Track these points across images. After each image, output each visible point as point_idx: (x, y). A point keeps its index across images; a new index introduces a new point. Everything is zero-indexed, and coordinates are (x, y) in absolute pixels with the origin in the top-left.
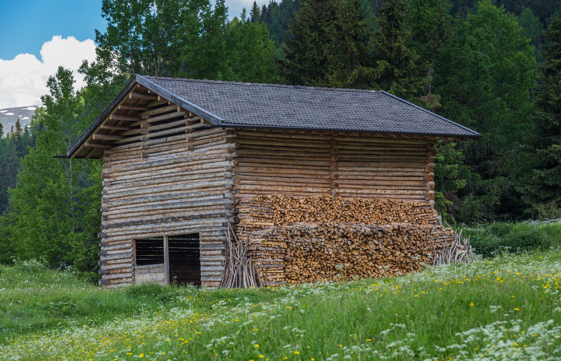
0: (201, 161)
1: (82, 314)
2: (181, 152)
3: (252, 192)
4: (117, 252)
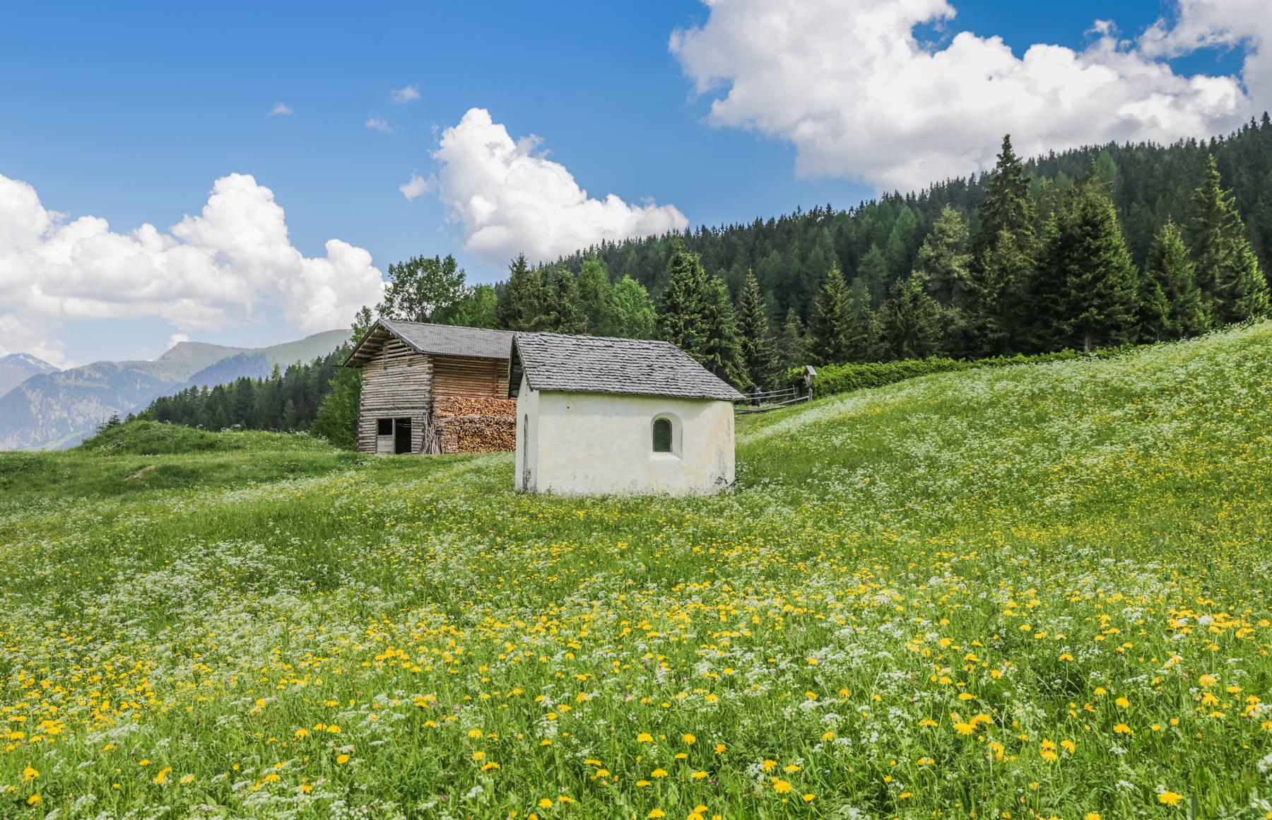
0: (414, 374)
1: (303, 470)
2: (404, 368)
3: (443, 394)
4: (368, 427)
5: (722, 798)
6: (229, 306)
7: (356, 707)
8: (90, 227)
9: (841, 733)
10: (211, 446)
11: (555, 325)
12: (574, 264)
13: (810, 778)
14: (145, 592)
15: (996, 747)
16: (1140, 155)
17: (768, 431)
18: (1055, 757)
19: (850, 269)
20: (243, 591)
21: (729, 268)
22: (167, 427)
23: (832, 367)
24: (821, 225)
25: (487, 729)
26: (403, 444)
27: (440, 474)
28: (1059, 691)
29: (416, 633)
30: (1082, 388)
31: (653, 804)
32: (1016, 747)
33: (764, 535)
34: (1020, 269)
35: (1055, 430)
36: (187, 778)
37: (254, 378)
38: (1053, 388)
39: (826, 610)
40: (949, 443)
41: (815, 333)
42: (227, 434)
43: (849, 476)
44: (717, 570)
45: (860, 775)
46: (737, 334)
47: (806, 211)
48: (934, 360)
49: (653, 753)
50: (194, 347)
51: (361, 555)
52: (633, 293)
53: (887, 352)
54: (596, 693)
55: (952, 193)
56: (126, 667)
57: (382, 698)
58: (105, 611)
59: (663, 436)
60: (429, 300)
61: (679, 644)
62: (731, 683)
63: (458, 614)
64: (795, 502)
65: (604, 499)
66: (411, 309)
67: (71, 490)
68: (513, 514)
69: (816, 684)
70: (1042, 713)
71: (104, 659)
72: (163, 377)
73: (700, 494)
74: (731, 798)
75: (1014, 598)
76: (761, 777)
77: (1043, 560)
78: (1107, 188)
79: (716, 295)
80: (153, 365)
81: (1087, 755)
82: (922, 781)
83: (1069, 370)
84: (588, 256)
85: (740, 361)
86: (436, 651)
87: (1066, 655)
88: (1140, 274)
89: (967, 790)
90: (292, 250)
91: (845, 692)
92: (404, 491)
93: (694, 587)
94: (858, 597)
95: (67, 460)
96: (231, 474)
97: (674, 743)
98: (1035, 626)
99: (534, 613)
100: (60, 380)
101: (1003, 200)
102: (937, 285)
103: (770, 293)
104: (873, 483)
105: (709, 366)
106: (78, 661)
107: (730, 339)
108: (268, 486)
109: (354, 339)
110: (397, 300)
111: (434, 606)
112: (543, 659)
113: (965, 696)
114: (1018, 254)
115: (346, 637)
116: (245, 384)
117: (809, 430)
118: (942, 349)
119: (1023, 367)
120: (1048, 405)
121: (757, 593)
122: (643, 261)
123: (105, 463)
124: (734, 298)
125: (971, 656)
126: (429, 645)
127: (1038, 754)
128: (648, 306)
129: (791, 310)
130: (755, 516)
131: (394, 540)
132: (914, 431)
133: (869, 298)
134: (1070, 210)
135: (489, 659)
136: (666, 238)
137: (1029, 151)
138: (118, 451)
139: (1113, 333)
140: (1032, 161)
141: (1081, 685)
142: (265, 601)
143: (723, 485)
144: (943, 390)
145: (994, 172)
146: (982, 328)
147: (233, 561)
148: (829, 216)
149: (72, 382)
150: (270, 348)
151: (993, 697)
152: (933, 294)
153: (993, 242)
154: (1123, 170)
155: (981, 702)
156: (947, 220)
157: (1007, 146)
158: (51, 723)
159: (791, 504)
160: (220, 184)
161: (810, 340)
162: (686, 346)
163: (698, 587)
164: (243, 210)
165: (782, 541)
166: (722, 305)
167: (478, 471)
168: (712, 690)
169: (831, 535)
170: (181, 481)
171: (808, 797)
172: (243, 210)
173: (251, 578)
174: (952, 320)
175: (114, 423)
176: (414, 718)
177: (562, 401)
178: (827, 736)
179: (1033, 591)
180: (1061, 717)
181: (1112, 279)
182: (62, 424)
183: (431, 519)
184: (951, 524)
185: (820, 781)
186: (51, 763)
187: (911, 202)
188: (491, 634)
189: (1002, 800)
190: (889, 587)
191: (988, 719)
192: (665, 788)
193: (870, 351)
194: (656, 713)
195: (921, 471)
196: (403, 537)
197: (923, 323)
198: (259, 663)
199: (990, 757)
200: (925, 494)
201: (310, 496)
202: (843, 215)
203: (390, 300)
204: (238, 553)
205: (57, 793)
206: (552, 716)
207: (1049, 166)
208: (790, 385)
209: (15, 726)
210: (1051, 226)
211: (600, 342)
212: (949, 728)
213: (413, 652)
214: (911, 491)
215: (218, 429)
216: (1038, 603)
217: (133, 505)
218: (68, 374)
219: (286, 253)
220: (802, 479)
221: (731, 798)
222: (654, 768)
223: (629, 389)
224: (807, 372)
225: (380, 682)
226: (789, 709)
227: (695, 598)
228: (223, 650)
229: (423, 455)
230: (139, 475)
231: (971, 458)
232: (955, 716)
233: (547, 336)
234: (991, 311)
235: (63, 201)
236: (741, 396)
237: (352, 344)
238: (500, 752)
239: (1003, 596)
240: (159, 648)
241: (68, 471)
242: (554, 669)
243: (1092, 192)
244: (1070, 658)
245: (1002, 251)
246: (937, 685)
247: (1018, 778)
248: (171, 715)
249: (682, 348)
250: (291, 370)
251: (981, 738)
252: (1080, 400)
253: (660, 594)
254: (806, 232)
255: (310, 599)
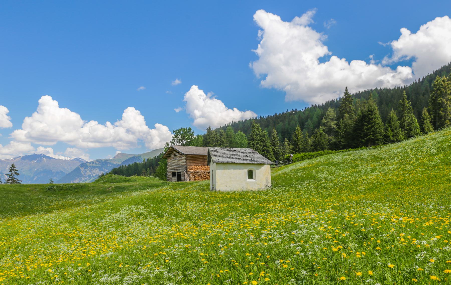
2: (178, 158)
5: (269, 269)
6: (131, 143)
7: (170, 248)
8: (93, 123)
9: (301, 252)
10: (128, 181)
11: (220, 145)
12: (225, 128)
13: (293, 264)
14: (114, 219)
15: (344, 255)
16: (384, 91)
17: (280, 172)
18: (360, 256)
19: (302, 126)
20: (139, 218)
21: (268, 127)
22: (115, 176)
23: (298, 154)
24: (294, 114)
25: (205, 253)
26: (179, 179)
27: (190, 187)
28: (361, 239)
29: (185, 229)
30: (368, 157)
31: (250, 271)
32: (349, 254)
33: (279, 200)
34: (350, 125)
35: (360, 169)
36: (127, 266)
37: (138, 162)
38: (360, 157)
39: (296, 219)
40: (331, 174)
41: (292, 145)
42: (133, 177)
43: (302, 184)
44: (267, 210)
45: (306, 262)
46: (271, 146)
47: (289, 111)
48: (326, 151)
49: (250, 258)
50: (122, 154)
51: (169, 209)
52: (241, 136)
53: (313, 149)
54: (234, 243)
55: (331, 104)
56: (110, 238)
57: (177, 245)
58: (104, 224)
59: (251, 175)
60: (184, 139)
61: (256, 230)
62: (271, 240)
63: (196, 223)
64: (288, 191)
65: (235, 192)
66: (180, 142)
67: (93, 193)
68: (210, 197)
69: (294, 239)
70: (357, 245)
71: (105, 236)
72: (115, 163)
73: (261, 190)
74: (271, 269)
75: (349, 215)
76: (280, 264)
77: (357, 204)
78: (375, 101)
79: (264, 136)
80: (112, 160)
81: (368, 255)
82: (323, 264)
83: (364, 152)
84: (228, 126)
85: (272, 153)
86: (190, 233)
87: (363, 229)
88: (384, 125)
89: (336, 266)
90: (147, 127)
91: (302, 241)
92: (179, 192)
93: (260, 215)
94: (305, 216)
95: (91, 185)
96: (134, 188)
97: (256, 256)
98: (355, 222)
99: (216, 223)
100: (88, 164)
101: (346, 105)
102: (327, 130)
103: (280, 134)
104: (309, 185)
105: (263, 155)
106: (98, 236)
107: (269, 147)
108: (144, 191)
109: (165, 151)
110: (176, 141)
111: (190, 221)
112: (219, 235)
113: (335, 241)
114: (350, 120)
115: (166, 230)
116: (136, 164)
117: (291, 171)
118: (329, 148)
119: (351, 152)
120: (359, 162)
121: (278, 216)
122: (244, 127)
123: (101, 185)
124: (270, 136)
125: (337, 231)
126: (189, 231)
127: (355, 256)
128: (245, 139)
129: (286, 139)
130: (277, 195)
131: (178, 204)
132: (321, 171)
133: (308, 134)
134: (365, 108)
135: (205, 235)
136: (250, 120)
137: (352, 91)
138: (104, 183)
139: (377, 142)
140: (353, 94)
141: (367, 237)
142: (145, 221)
143: (268, 187)
144: (329, 159)
145: (343, 97)
146: (340, 142)
147: (136, 211)
148: (296, 112)
149: (91, 165)
150: (142, 154)
151: (343, 241)
152: (326, 133)
153: (343, 117)
154: (379, 96)
155: (340, 243)
156: (330, 112)
157: (346, 90)
158: (92, 252)
159: (287, 192)
160: (126, 111)
161: (291, 147)
162: (257, 150)
163: (261, 215)
164: (133, 117)
165: (284, 202)
166: (266, 138)
167: (200, 185)
168: (266, 242)
169: (298, 200)
170: (121, 190)
171: (292, 269)
172: (133, 117)
173: (141, 215)
174: (331, 140)
175: (103, 175)
176: (186, 250)
177: (222, 166)
178: (297, 253)
179: (354, 213)
180: (362, 246)
181: (376, 126)
182: (89, 176)
183: (187, 199)
184: (331, 196)
185: (295, 264)
186: (93, 262)
187: (319, 107)
188: (205, 228)
189: (345, 268)
190: (314, 213)
191: (341, 247)
192: (253, 267)
193: (308, 149)
194: (251, 248)
195: (323, 182)
196: (180, 204)
197: (323, 141)
198: (144, 237)
199: (342, 257)
200: (324, 188)
201: (155, 193)
202: (300, 111)
203: (174, 140)
204: (137, 208)
205: (95, 269)
206: (222, 249)
207: (358, 95)
208: (286, 159)
209: (84, 252)
210: (359, 112)
211: (232, 149)
212: (331, 250)
213: (184, 233)
214: (320, 187)
215: (130, 176)
216: (355, 216)
217: (109, 197)
218: (90, 163)
219: (145, 128)
220: (289, 185)
221: (271, 269)
222: (250, 262)
223: (241, 162)
224: (290, 156)
225: (176, 241)
226: (287, 246)
227: (260, 218)
228: (134, 234)
229: (185, 182)
230: (110, 189)
231: (337, 177)
232: (333, 247)
233: (217, 148)
234: (342, 137)
235: (86, 118)
236: (272, 163)
237: (164, 152)
238: (209, 259)
239: (346, 215)
240: (118, 233)
241: (92, 188)
242: (222, 237)
243: (371, 102)
244: (364, 230)
245: (345, 120)
246: (327, 239)
247: (350, 262)
248: (122, 250)
249: (255, 150)
250: (148, 160)
251: (340, 252)
252: (367, 161)
253: (251, 217)
254: (289, 116)
255: (156, 220)
